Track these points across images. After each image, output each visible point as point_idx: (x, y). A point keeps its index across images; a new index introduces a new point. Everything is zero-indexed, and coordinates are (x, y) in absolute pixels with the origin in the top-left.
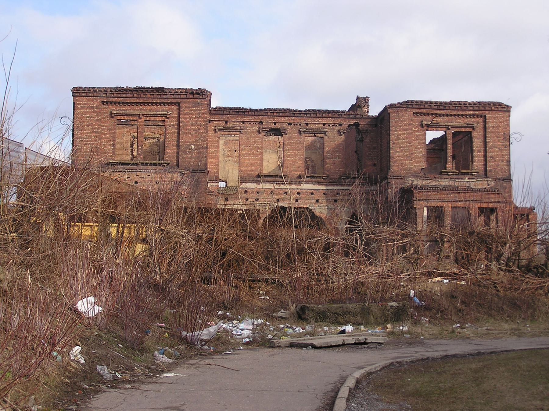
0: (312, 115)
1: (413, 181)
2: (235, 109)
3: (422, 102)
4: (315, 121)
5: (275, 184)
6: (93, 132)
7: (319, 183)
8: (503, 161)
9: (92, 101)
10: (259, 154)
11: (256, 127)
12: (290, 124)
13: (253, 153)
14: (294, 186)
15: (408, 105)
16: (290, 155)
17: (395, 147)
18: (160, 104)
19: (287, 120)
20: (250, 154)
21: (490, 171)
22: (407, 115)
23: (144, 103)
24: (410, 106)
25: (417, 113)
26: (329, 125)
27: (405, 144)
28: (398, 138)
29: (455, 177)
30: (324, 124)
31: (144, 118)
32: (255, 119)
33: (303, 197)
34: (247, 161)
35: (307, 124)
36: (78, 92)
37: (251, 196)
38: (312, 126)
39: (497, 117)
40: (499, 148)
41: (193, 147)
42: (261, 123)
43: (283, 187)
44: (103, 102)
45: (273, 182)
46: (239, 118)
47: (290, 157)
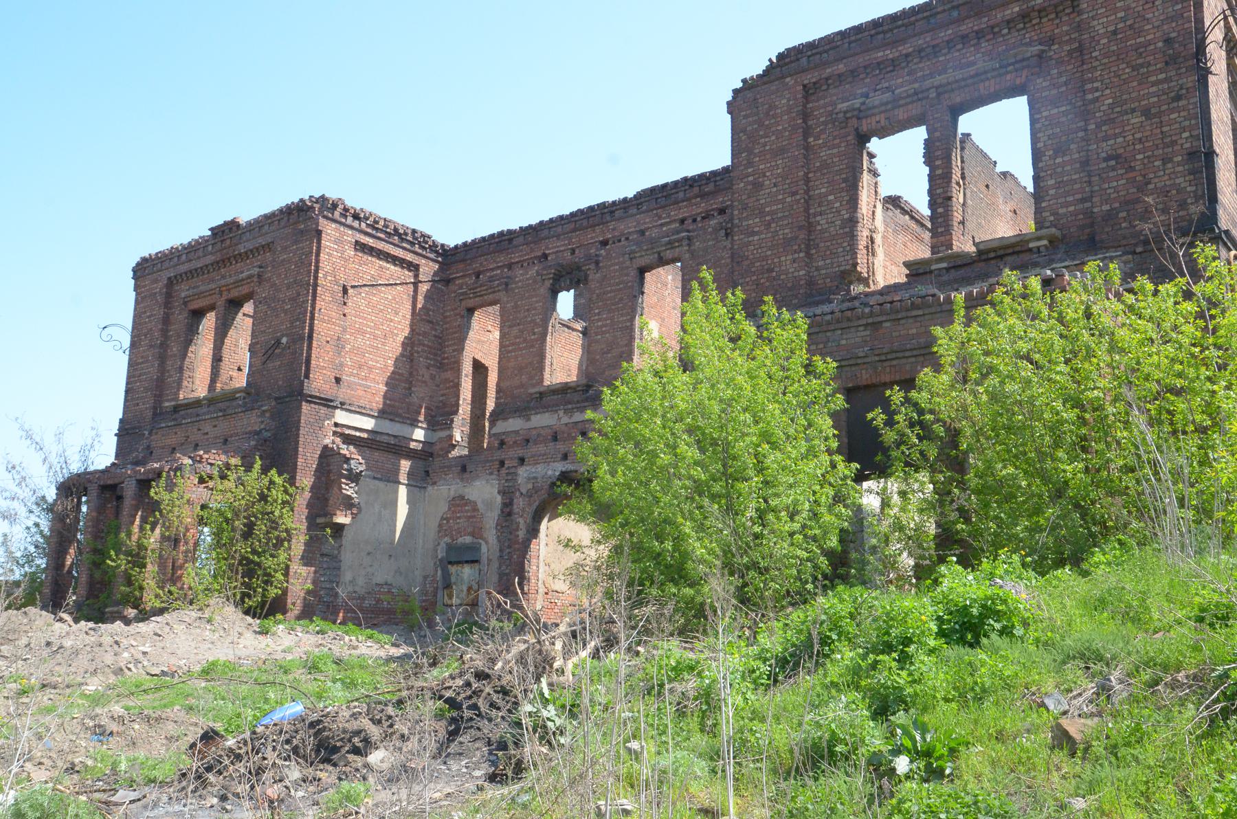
4: (660, 218)
5: (561, 413)
6: (151, 346)
8: (1165, 161)
9: (156, 281)
10: (536, 340)
12: (604, 243)
13: (525, 340)
16: (601, 327)
17: (747, 218)
19: (597, 235)
20: (519, 343)
21: (1110, 216)
26: (695, 221)
27: (778, 202)
28: (757, 186)
30: (682, 221)
32: (532, 250)
35: (642, 233)
40: (1146, 113)
41: (284, 340)
42: (545, 256)
46: (502, 259)
47: (603, 333)
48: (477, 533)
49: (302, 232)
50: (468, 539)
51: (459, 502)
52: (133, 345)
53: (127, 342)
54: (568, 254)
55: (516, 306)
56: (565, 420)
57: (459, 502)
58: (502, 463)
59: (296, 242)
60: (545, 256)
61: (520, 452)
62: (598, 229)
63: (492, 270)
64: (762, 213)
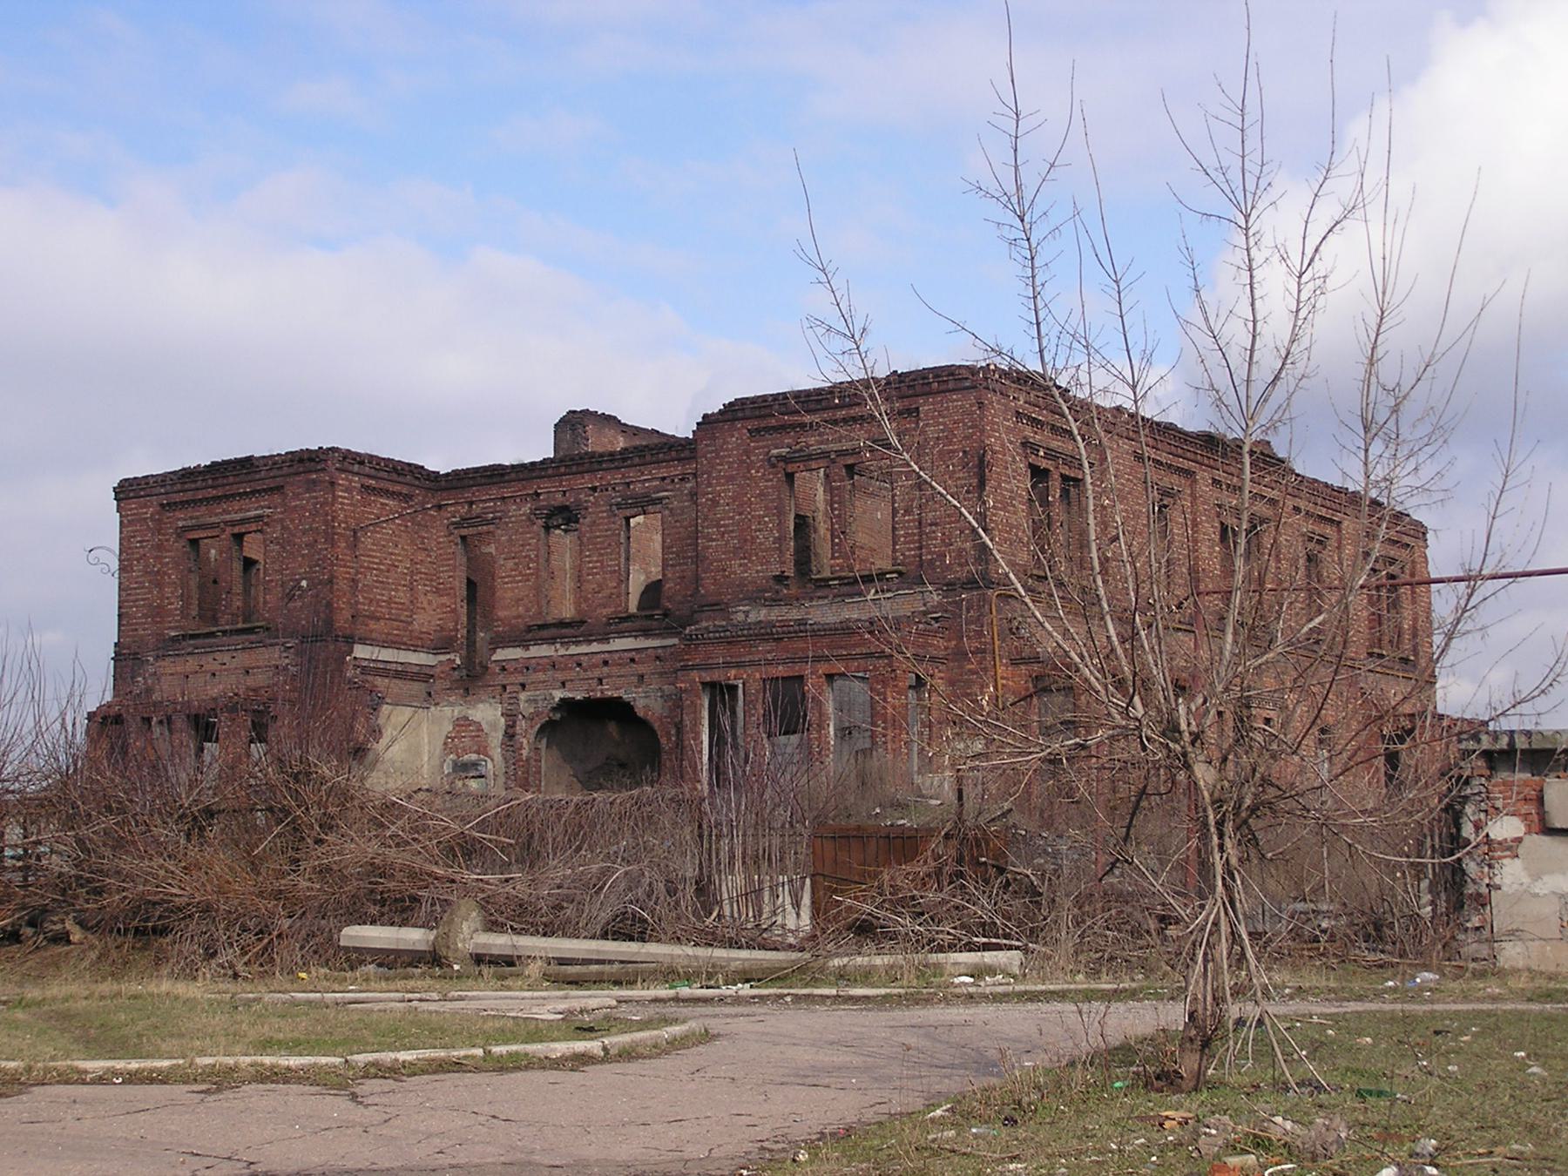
0: (637, 460)
1: (747, 613)
2: (485, 469)
3: (764, 398)
7: (646, 633)
9: (146, 506)
11: (526, 509)
12: (594, 489)
14: (595, 647)
15: (737, 411)
18: (253, 492)
19: (586, 481)
22: (735, 439)
23: (226, 497)
24: (740, 415)
25: (758, 430)
28: (715, 503)
29: (845, 589)
30: (664, 479)
31: (229, 530)
33: (615, 670)
34: (509, 594)
36: (127, 492)
37: (512, 679)
38: (638, 488)
39: (947, 408)
41: (304, 583)
43: (574, 650)
44: (162, 505)
45: (551, 641)
46: (494, 492)
48: (482, 750)
49: (314, 481)
50: (474, 757)
51: (463, 723)
52: (122, 569)
53: (115, 565)
54: (559, 496)
55: (510, 540)
56: (562, 652)
57: (463, 723)
58: (504, 687)
59: (308, 491)
60: (538, 495)
61: (521, 679)
62: (587, 476)
63: (485, 501)
64: (718, 526)
